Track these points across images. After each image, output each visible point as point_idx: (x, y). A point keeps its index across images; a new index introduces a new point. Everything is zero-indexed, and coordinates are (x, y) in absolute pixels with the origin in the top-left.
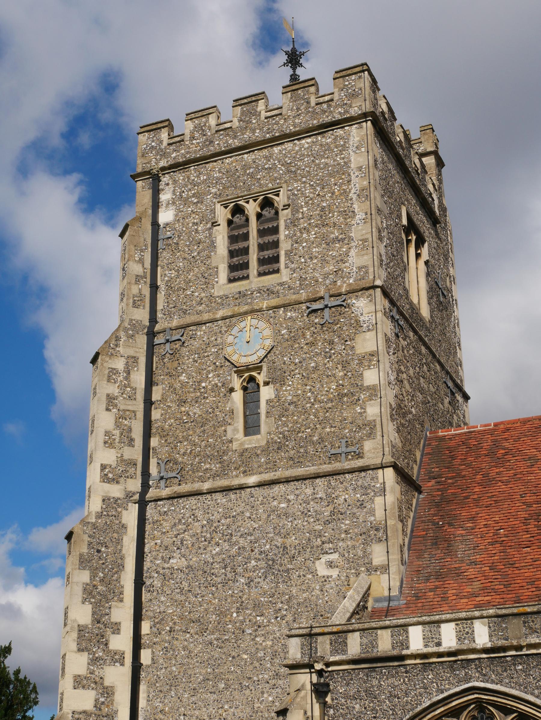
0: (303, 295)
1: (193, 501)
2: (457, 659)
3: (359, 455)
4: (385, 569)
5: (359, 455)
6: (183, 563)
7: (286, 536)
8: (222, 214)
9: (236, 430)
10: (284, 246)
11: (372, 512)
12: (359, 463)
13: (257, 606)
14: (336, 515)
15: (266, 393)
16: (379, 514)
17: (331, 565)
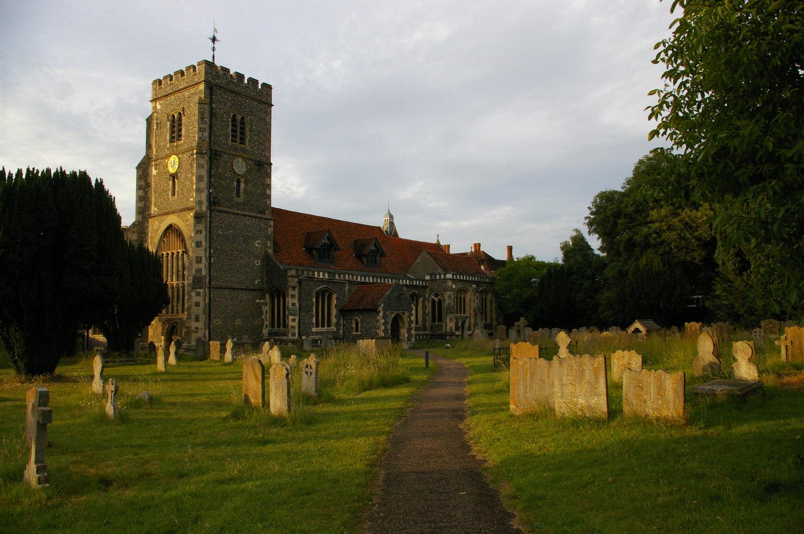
0: (252, 157)
1: (225, 215)
2: (322, 281)
3: (265, 214)
4: (270, 248)
5: (265, 214)
6: (222, 233)
7: (249, 233)
8: (232, 114)
9: (234, 194)
10: (248, 138)
11: (268, 231)
12: (264, 217)
13: (241, 251)
14: (260, 230)
15: (242, 185)
16: (270, 233)
17: (259, 243)
